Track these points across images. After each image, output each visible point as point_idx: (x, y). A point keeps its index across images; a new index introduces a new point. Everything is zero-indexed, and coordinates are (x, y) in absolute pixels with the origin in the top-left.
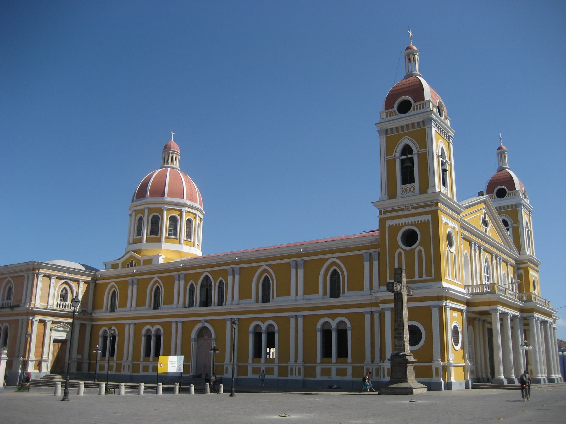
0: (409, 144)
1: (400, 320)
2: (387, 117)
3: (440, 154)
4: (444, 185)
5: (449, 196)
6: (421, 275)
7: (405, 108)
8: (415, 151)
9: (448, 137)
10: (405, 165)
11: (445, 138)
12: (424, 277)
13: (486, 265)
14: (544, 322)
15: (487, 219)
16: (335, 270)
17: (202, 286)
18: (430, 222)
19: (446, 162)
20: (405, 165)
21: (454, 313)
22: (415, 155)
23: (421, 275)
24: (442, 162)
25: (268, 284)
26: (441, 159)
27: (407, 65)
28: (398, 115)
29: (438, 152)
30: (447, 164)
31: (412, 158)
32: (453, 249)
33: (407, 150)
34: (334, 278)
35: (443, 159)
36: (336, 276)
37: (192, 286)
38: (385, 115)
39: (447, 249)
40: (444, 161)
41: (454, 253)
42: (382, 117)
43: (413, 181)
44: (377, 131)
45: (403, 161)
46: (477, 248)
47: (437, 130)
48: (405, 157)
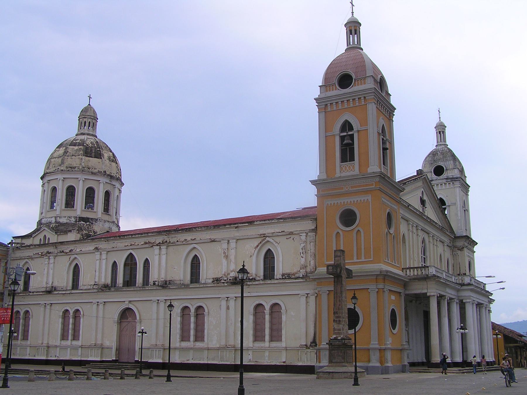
1: (339, 303)
3: (381, 132)
4: (384, 164)
6: (359, 256)
9: (389, 114)
10: (345, 142)
11: (386, 115)
12: (363, 259)
13: (423, 246)
14: (479, 305)
15: (425, 198)
16: (269, 250)
17: (125, 265)
19: (387, 139)
20: (345, 142)
21: (392, 296)
23: (359, 256)
24: (383, 139)
25: (198, 263)
27: (348, 37)
28: (338, 89)
30: (388, 142)
31: (353, 135)
32: (392, 231)
33: (347, 126)
34: (268, 258)
35: (384, 137)
36: (270, 256)
37: (115, 264)
39: (386, 230)
40: (385, 139)
41: (393, 234)
43: (352, 159)
44: (317, 105)
45: (342, 138)
46: (414, 228)
48: (345, 134)
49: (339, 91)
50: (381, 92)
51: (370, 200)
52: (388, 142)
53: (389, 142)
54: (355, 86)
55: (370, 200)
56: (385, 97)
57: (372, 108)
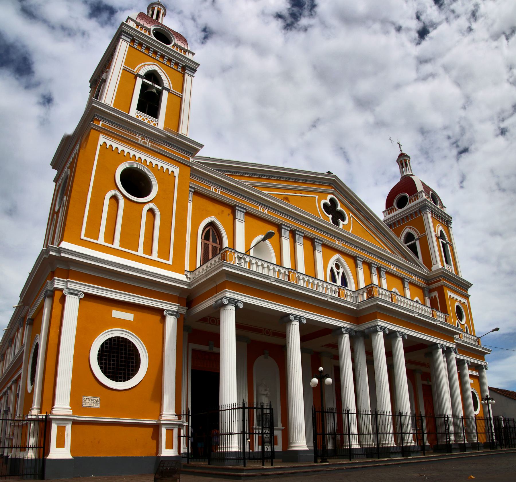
0: (410, 232)
2: (389, 214)
3: (439, 236)
4: (447, 263)
5: (454, 273)
7: (402, 203)
8: (416, 237)
9: (446, 222)
18: (437, 298)
19: (447, 243)
22: (417, 240)
24: (443, 243)
26: (440, 240)
28: (398, 210)
29: (437, 234)
30: (448, 245)
31: (415, 244)
32: (463, 322)
33: (409, 237)
38: (387, 213)
41: (466, 325)
42: (385, 215)
47: (433, 216)
49: (398, 211)
50: (433, 203)
51: (437, 297)
52: (448, 245)
53: (449, 245)
54: (410, 203)
55: (437, 297)
56: (440, 208)
57: (429, 217)
